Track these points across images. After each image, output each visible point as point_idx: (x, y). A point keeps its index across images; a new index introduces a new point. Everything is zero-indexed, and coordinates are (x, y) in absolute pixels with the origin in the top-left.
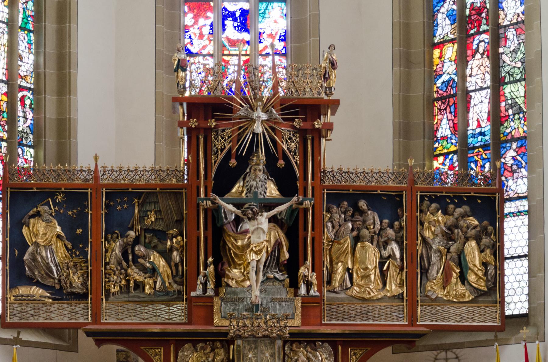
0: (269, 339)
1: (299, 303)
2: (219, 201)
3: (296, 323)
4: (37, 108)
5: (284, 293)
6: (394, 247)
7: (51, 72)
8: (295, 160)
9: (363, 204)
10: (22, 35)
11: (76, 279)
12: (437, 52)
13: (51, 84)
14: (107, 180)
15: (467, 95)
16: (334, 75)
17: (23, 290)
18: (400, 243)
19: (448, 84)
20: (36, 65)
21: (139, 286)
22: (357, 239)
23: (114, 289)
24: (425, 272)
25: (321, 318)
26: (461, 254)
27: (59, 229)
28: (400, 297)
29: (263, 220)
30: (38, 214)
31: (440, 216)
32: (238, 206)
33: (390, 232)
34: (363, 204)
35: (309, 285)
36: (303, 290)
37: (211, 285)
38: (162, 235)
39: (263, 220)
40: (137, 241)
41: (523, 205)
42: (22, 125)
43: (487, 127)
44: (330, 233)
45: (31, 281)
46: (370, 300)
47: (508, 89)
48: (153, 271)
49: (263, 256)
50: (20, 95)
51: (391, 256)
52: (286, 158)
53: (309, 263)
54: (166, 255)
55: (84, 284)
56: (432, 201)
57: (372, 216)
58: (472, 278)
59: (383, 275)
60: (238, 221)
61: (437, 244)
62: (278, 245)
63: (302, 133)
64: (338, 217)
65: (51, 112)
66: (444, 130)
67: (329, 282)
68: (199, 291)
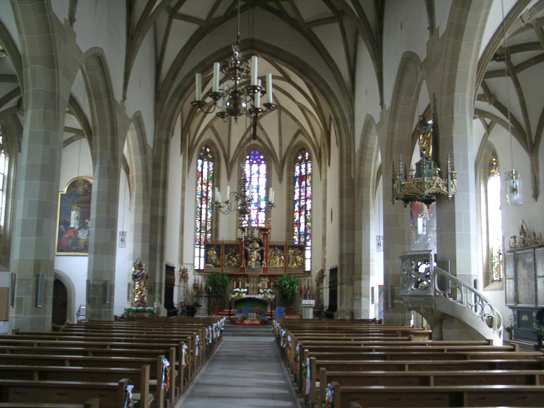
0: (256, 276)
1: (262, 269)
2: (247, 248)
3: (262, 273)
4: (211, 225)
5: (259, 267)
6: (283, 257)
7: (214, 218)
8: (262, 239)
9: (276, 248)
10: (209, 210)
11: (218, 263)
12: (295, 214)
13: (214, 220)
14: (225, 243)
15: (300, 224)
16: (270, 223)
17: (207, 265)
18: (283, 255)
19: (297, 221)
20: (212, 217)
21: (231, 264)
22: (275, 255)
23: (226, 265)
24: (288, 262)
25: (267, 271)
26: (296, 258)
27: (215, 253)
28: (283, 267)
29: (255, 252)
30: (211, 250)
31: (292, 251)
32: (251, 249)
33: (282, 254)
34: (276, 248)
35: (264, 265)
36: (263, 266)
37: (245, 265)
38: (236, 254)
39: (255, 252)
40: (230, 255)
41: (309, 248)
42: (208, 229)
43: (304, 231)
44: (269, 254)
45: (209, 263)
46: (277, 268)
47: (308, 224)
48: (233, 261)
49: (255, 259)
50: (208, 223)
51: (282, 259)
52: (260, 239)
53: (265, 260)
54: (236, 258)
55: (220, 264)
56: (291, 247)
57: (278, 250)
58: (298, 264)
59: (280, 263)
60: (251, 252)
61: (291, 256)
62: (258, 257)
63: (264, 234)
64: (271, 251)
65: (214, 226)
66: (296, 230)
67: (269, 264)
68: (242, 266)
